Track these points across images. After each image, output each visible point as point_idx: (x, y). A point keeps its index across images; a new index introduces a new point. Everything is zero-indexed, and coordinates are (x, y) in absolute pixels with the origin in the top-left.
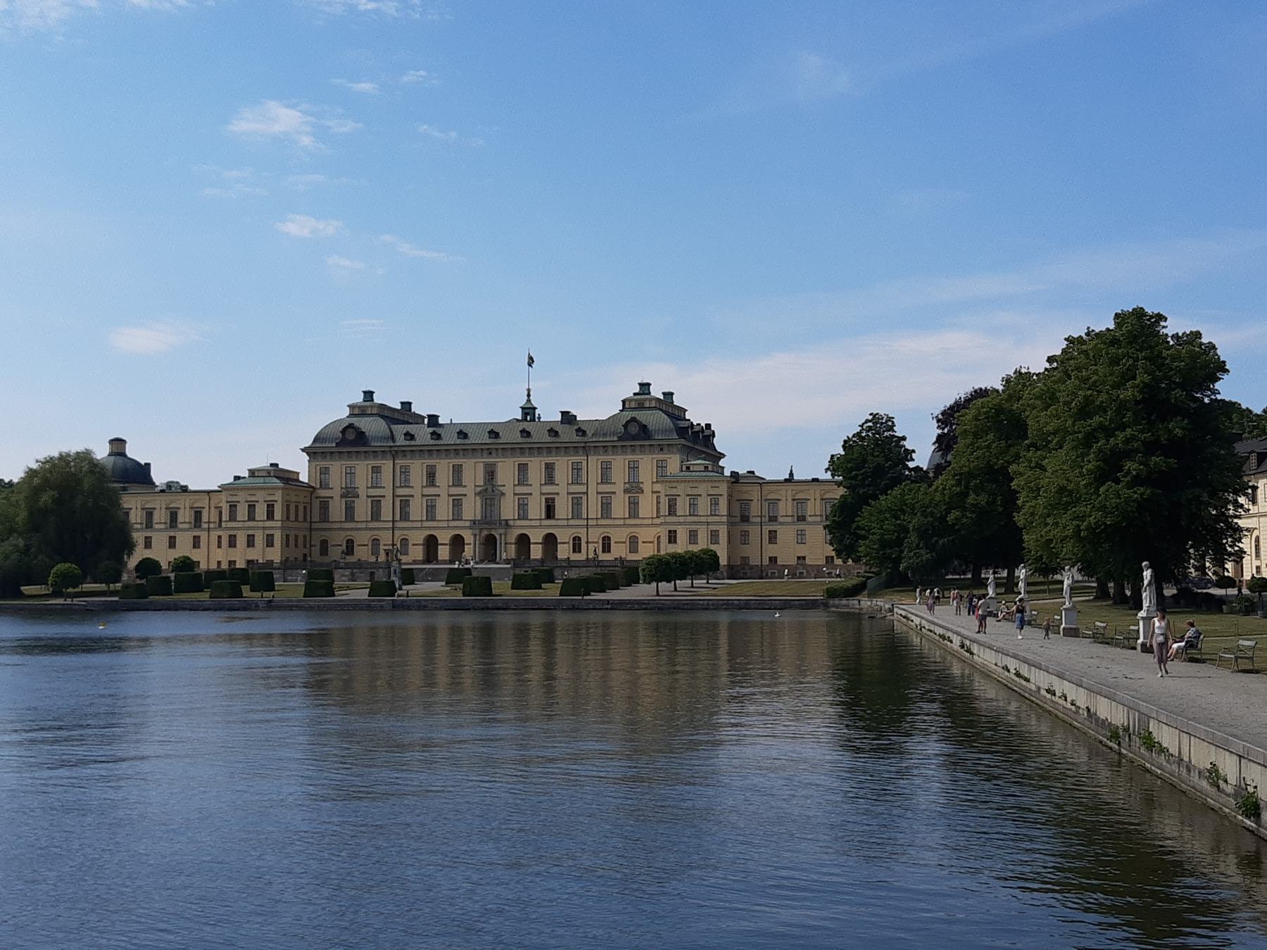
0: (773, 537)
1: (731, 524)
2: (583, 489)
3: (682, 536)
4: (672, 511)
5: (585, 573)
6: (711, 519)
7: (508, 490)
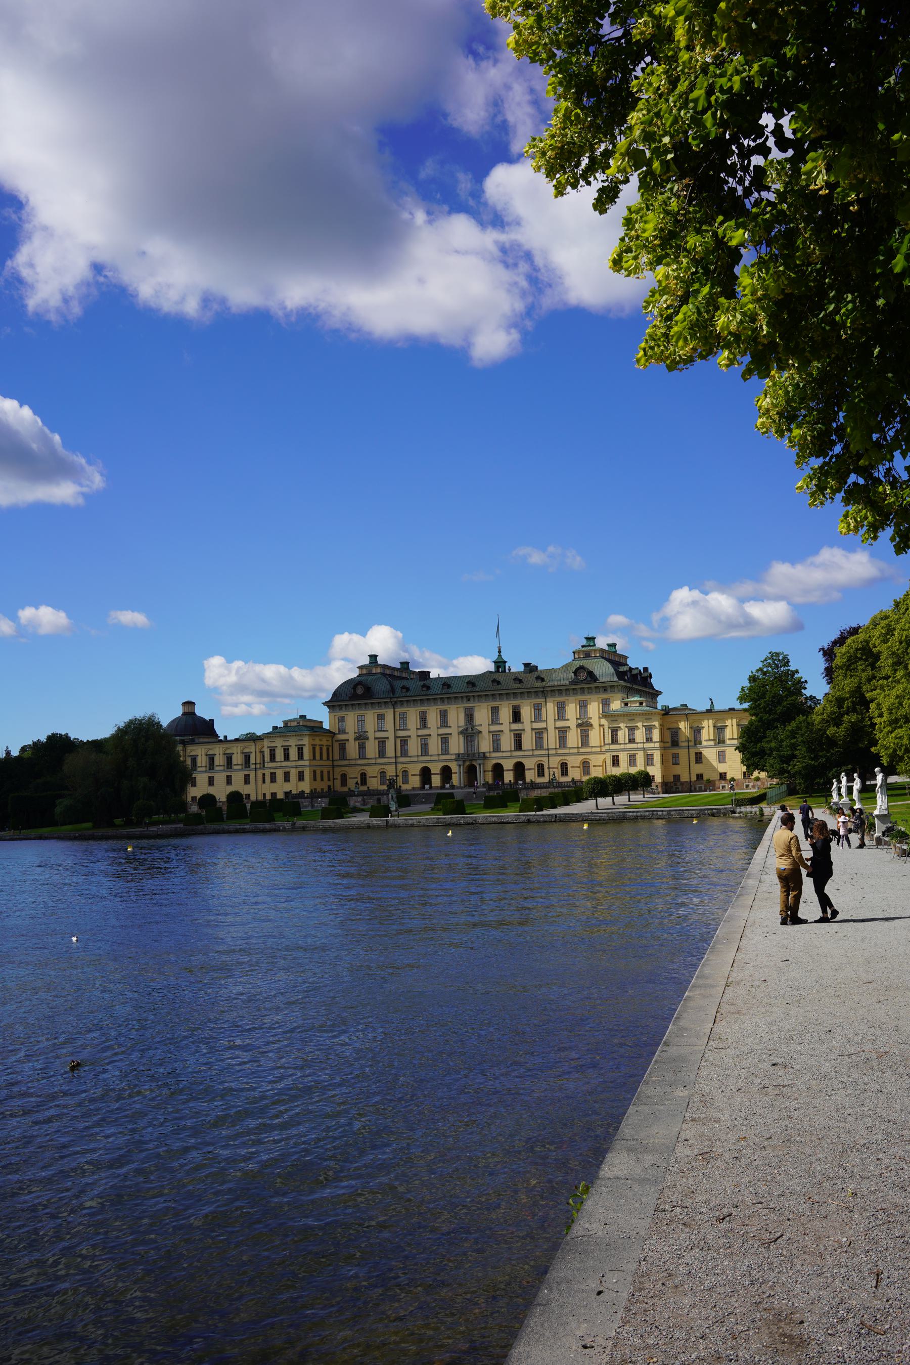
0: (699, 757)
1: (664, 749)
2: (543, 725)
3: (623, 758)
5: (544, 793)
7: (484, 729)
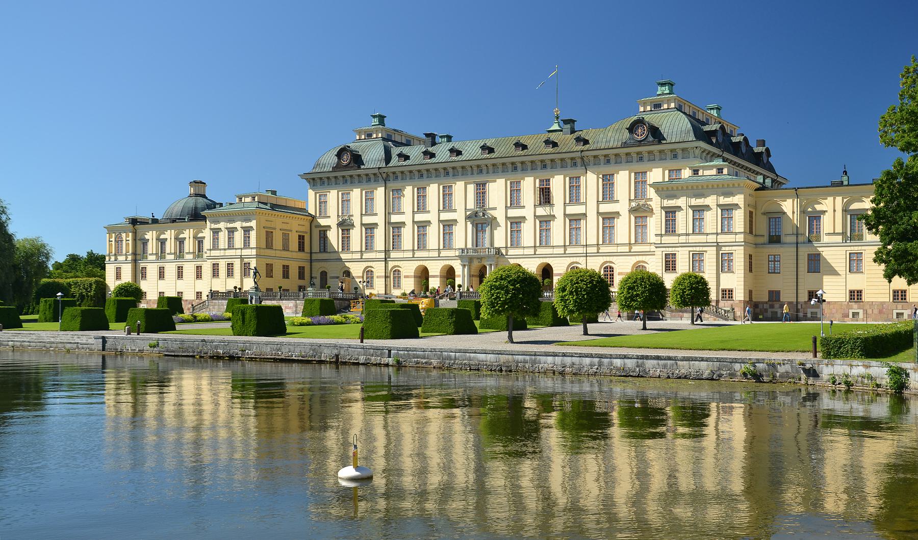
4: (670, 228)
6: (722, 238)
